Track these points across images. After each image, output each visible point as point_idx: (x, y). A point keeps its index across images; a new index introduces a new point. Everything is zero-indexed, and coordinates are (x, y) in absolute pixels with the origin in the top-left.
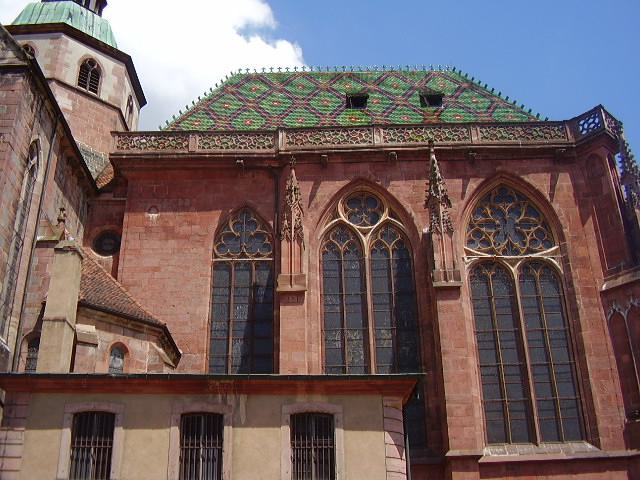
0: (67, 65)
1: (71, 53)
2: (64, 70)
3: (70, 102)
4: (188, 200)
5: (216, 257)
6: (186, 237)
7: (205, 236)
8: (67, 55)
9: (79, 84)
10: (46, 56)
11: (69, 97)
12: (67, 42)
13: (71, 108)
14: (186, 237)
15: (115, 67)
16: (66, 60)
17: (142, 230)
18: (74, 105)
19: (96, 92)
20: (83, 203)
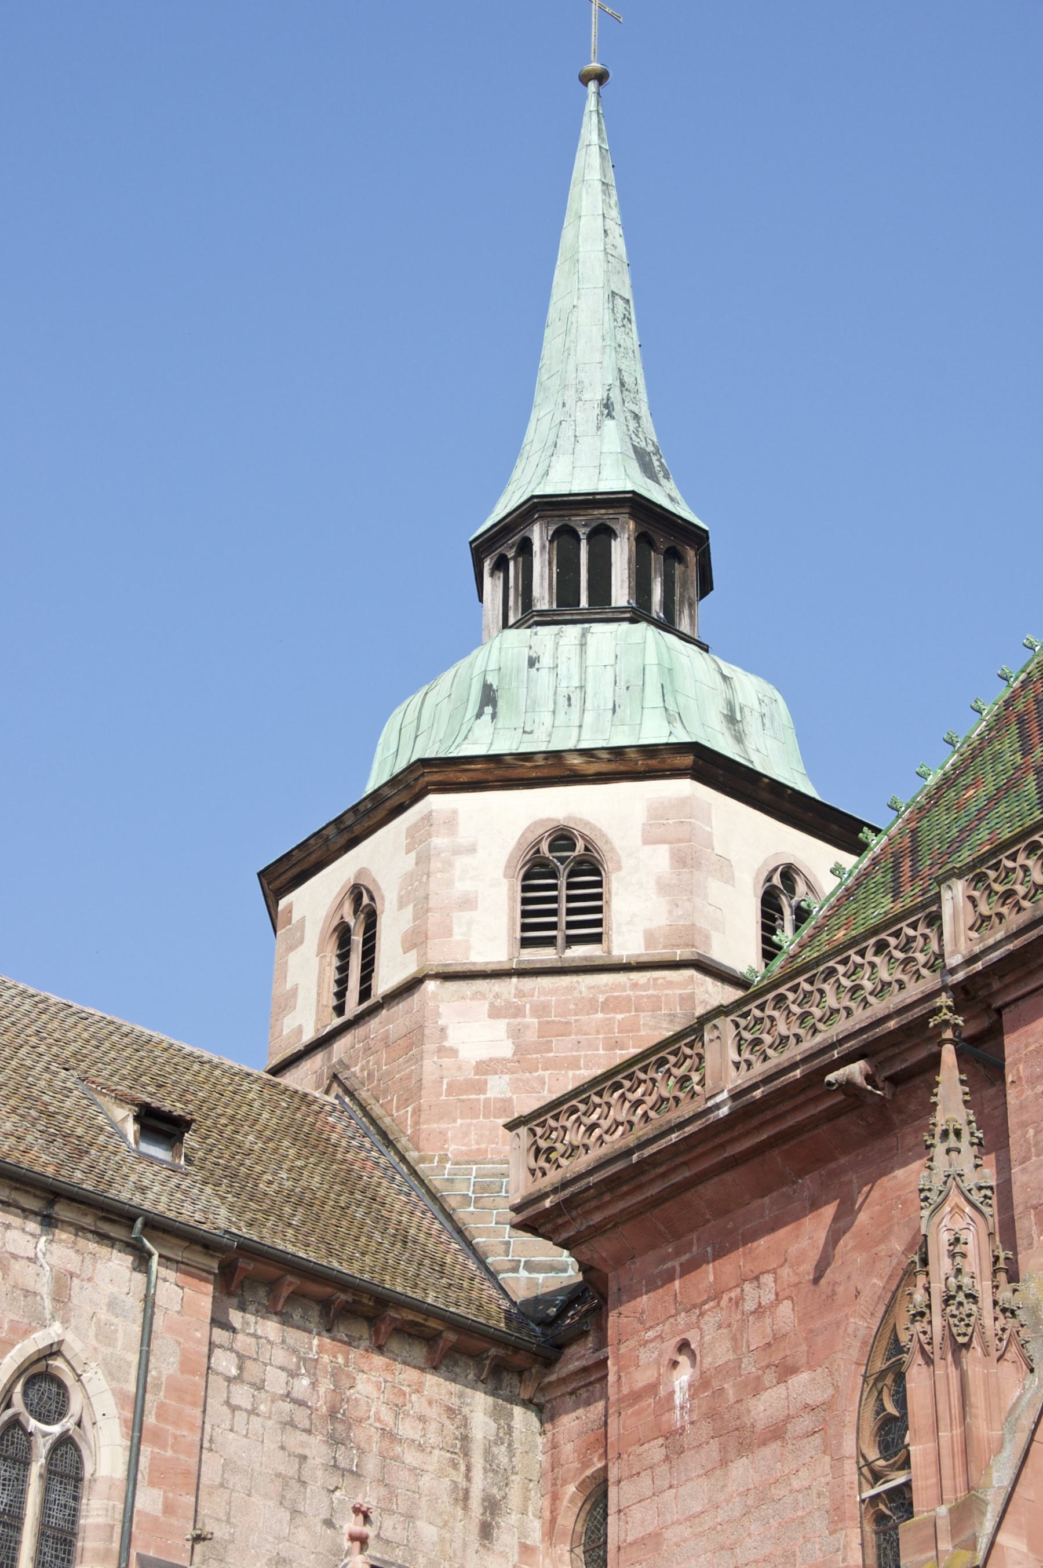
0: (468, 903)
1: (472, 850)
2: (460, 921)
3: (501, 1025)
4: (768, 1279)
5: (877, 1477)
6: (776, 1432)
7: (828, 1405)
8: (461, 862)
9: (526, 943)
10: (401, 905)
11: (495, 1013)
12: (451, 821)
13: (506, 1050)
14: (776, 1432)
15: (657, 813)
16: (461, 887)
17: (655, 1450)
18: (515, 1033)
19: (597, 939)
20: (496, 1414)
